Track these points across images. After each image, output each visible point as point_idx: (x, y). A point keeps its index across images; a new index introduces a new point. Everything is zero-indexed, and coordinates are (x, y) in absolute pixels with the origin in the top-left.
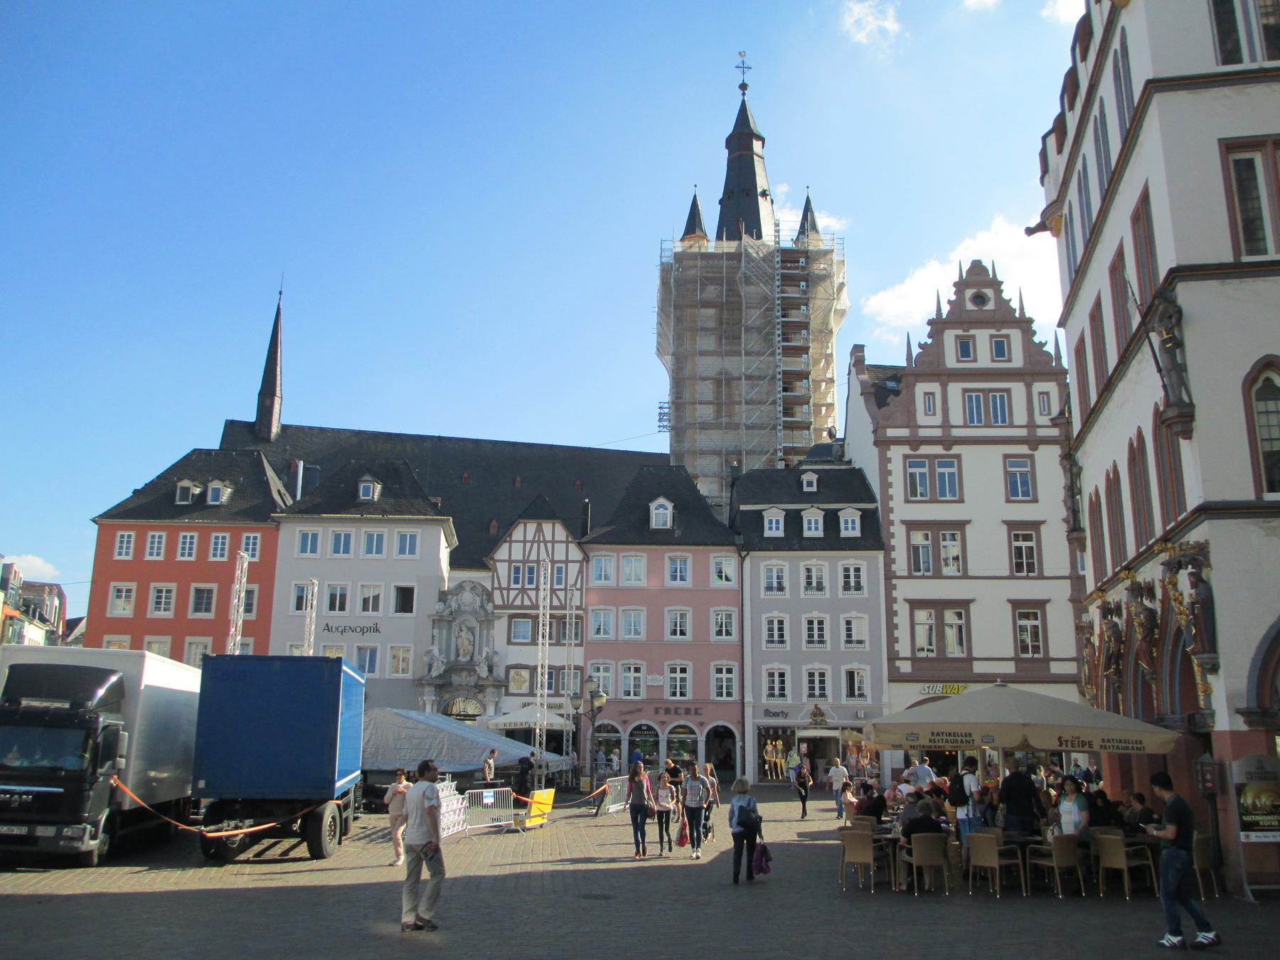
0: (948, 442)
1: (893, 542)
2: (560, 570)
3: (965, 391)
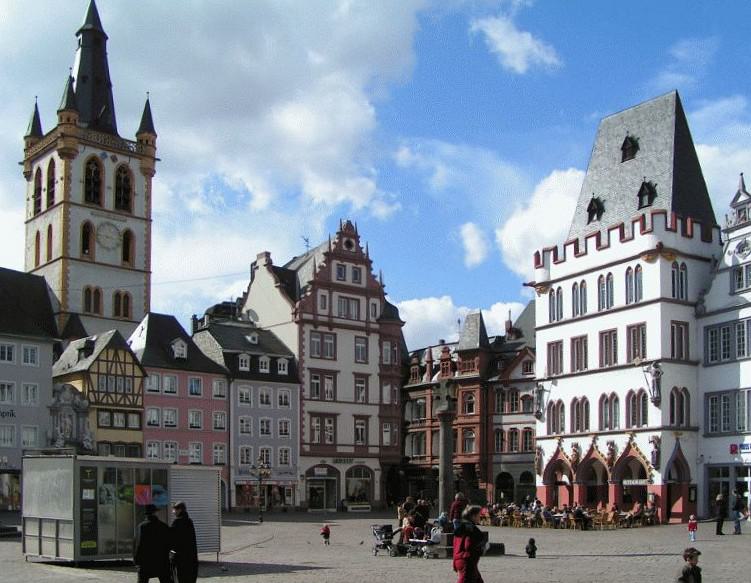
0: (331, 325)
1: (304, 379)
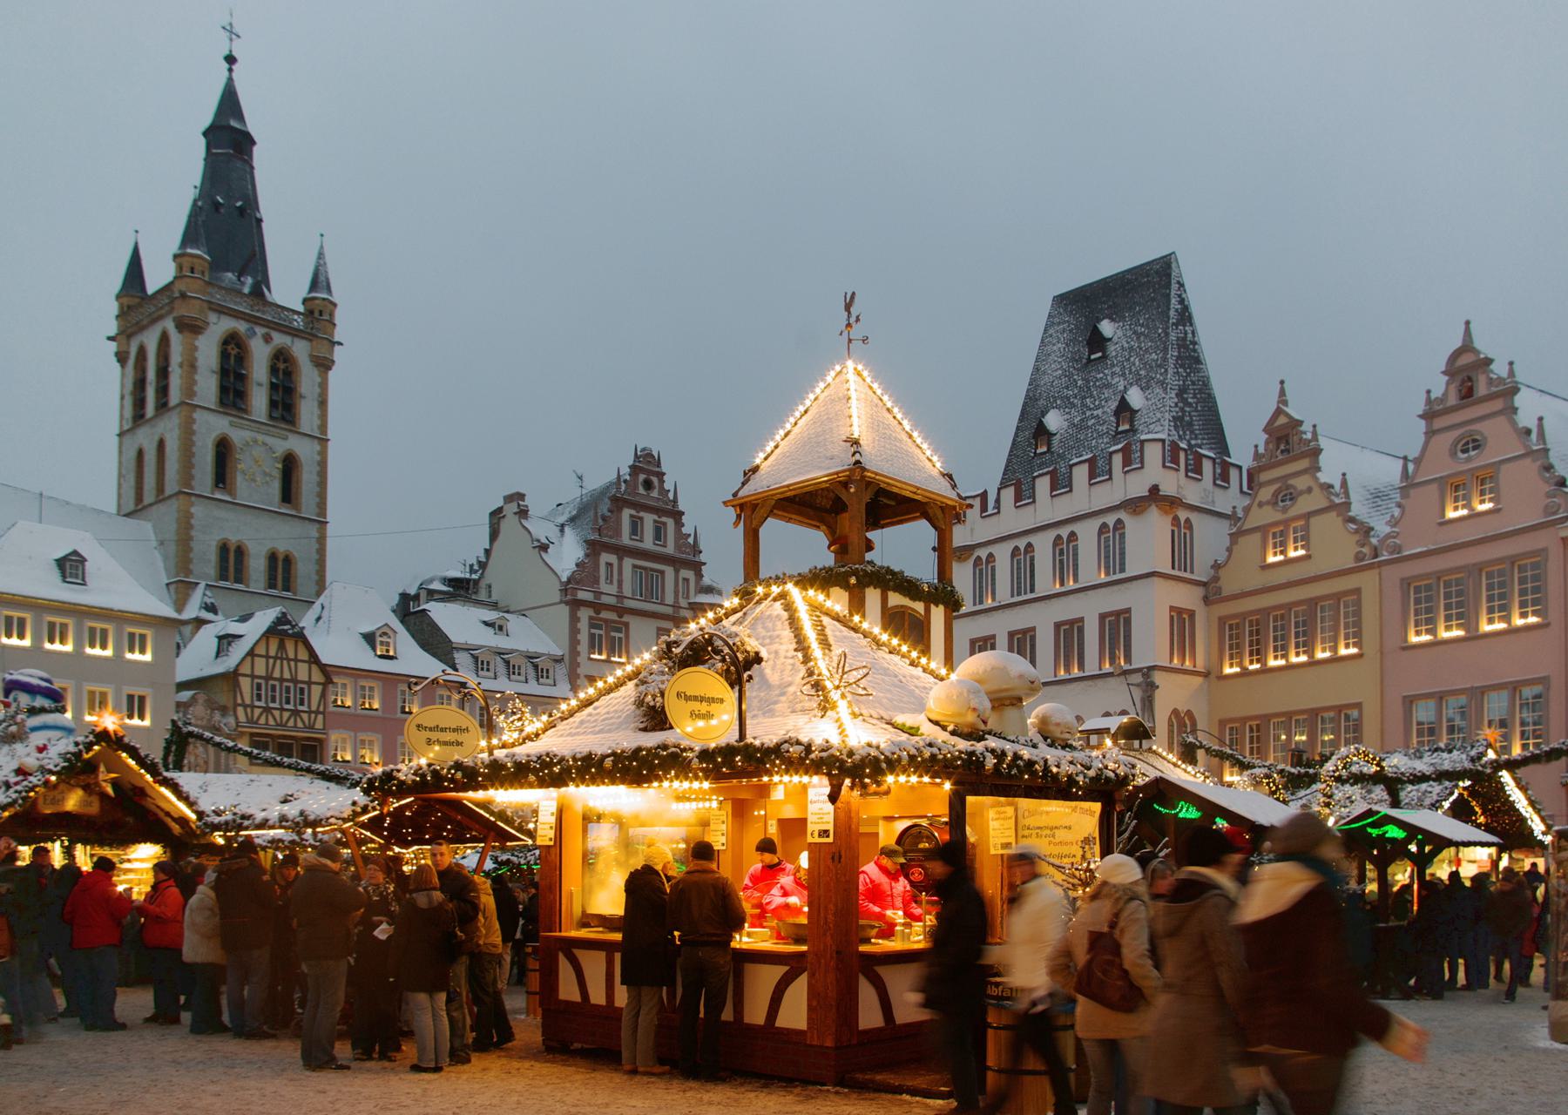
0: (622, 611)
2: (302, 690)
3: (635, 566)
